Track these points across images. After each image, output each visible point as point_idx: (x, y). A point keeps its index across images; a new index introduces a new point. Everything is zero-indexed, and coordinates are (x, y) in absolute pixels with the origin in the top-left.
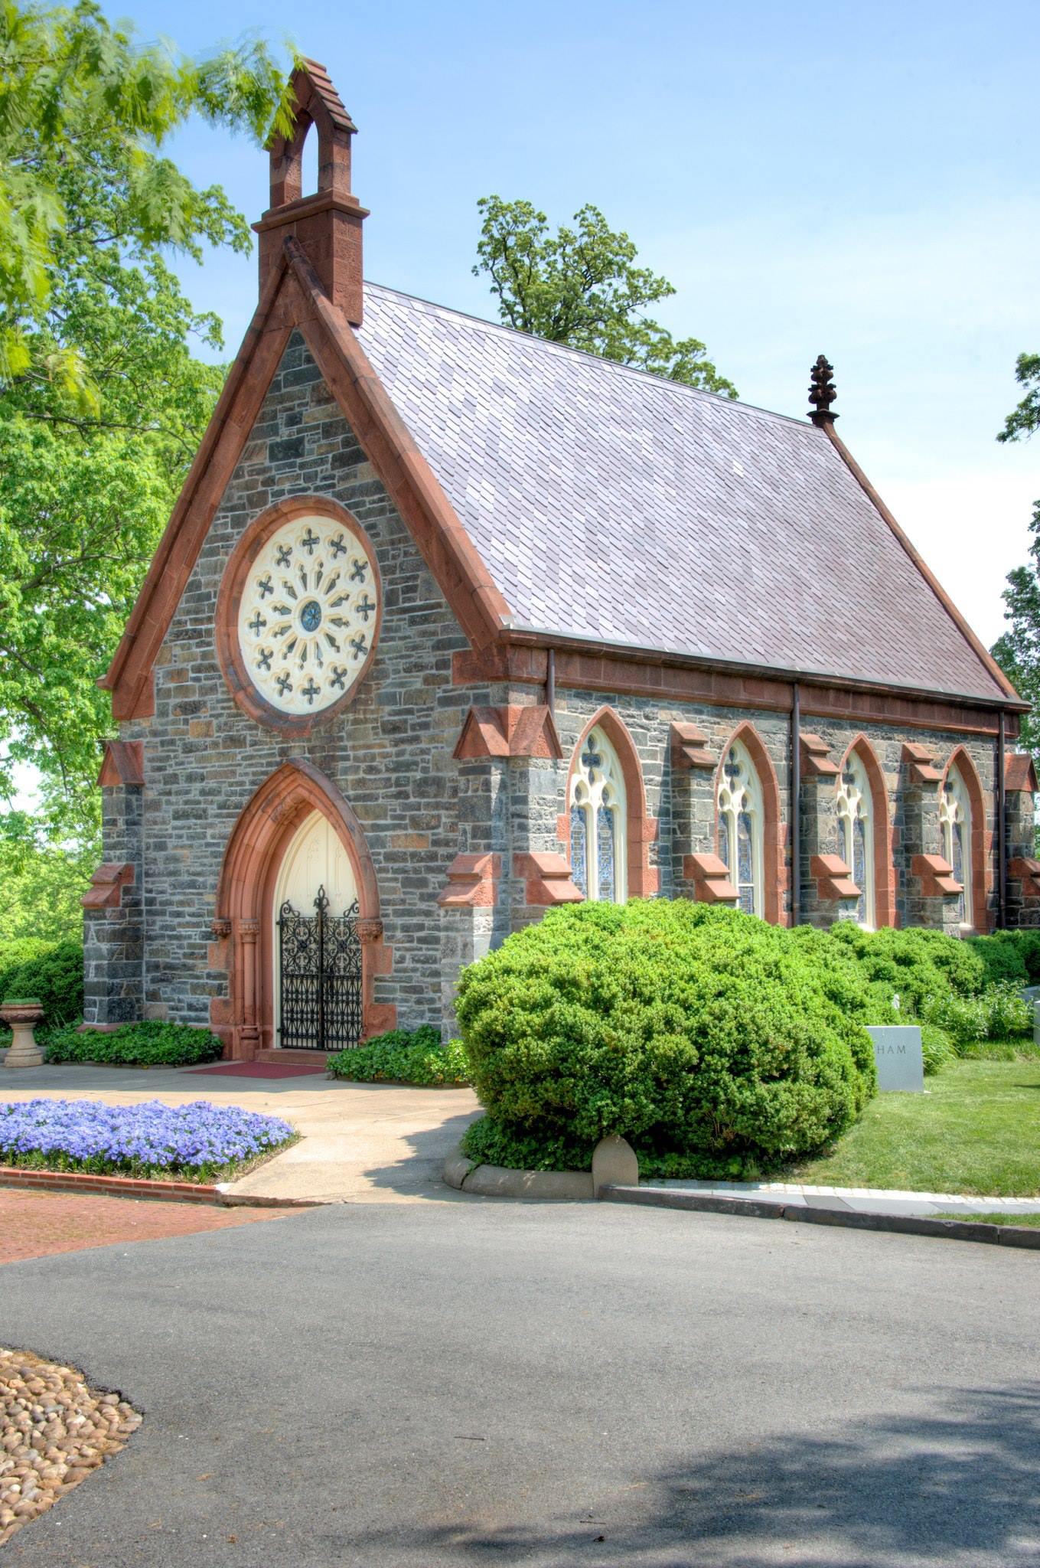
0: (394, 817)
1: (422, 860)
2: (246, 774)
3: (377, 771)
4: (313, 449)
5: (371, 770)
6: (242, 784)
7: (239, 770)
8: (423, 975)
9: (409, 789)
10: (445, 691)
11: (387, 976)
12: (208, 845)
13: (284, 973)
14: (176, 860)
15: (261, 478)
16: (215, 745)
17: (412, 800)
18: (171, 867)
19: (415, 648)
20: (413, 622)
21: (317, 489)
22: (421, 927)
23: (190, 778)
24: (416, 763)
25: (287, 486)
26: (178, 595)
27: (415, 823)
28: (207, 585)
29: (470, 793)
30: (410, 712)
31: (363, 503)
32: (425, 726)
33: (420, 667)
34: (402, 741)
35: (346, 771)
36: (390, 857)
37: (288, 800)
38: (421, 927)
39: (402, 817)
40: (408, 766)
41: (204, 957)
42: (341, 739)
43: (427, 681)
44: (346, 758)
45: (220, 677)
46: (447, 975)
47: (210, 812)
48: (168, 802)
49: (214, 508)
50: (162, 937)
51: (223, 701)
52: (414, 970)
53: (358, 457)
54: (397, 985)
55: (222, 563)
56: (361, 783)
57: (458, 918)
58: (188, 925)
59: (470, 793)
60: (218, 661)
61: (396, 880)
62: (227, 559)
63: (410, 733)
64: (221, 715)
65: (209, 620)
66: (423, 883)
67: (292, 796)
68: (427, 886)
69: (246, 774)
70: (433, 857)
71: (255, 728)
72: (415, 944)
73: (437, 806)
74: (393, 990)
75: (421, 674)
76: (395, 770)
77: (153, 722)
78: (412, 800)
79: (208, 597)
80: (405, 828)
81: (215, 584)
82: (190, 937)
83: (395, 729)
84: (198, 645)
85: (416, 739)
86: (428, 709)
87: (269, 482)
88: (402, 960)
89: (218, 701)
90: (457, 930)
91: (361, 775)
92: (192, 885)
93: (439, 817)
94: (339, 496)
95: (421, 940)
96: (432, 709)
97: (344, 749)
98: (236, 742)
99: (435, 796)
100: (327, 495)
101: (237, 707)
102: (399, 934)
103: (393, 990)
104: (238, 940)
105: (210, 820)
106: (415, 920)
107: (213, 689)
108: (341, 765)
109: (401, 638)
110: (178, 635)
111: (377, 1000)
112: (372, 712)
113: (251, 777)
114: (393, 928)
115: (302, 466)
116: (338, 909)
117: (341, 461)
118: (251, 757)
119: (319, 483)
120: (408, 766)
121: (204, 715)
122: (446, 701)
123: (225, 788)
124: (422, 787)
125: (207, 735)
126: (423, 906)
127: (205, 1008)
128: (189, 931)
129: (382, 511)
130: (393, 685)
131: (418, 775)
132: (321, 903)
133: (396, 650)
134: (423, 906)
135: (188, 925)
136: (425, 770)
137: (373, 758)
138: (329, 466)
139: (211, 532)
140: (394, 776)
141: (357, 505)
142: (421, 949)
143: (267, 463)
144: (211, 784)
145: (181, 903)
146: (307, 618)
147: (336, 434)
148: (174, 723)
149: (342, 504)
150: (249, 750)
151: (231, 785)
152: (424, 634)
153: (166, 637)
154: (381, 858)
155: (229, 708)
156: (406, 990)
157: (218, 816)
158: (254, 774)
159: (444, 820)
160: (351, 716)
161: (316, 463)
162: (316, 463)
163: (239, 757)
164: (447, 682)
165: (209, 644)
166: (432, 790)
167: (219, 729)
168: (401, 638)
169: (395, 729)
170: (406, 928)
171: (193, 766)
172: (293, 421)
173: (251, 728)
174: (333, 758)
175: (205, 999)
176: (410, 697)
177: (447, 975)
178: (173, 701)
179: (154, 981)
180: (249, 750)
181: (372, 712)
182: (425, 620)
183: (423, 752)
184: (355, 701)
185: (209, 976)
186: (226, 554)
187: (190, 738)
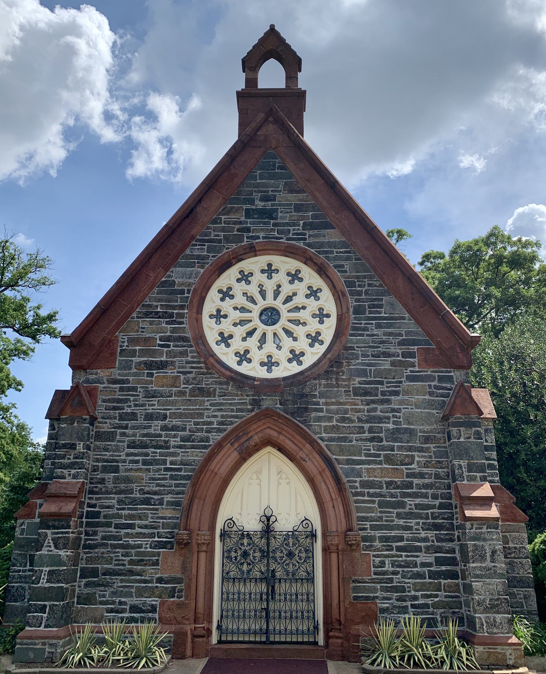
0: (367, 455)
1: (398, 487)
2: (215, 416)
3: (351, 421)
4: (283, 217)
5: (343, 420)
6: (211, 423)
7: (206, 413)
8: (403, 577)
9: (382, 435)
10: (411, 372)
11: (366, 578)
12: (166, 469)
13: (225, 578)
14: (128, 480)
15: (237, 227)
16: (182, 393)
17: (385, 443)
18: (122, 486)
19: (382, 342)
20: (379, 326)
21: (288, 239)
22: (401, 539)
23: (149, 417)
24: (388, 418)
25: (262, 235)
26: (152, 288)
27: (389, 460)
28: (182, 284)
29: (462, 440)
30: (381, 383)
31: (332, 252)
32: (397, 393)
33: (386, 355)
34: (373, 402)
35: (319, 419)
36: (364, 484)
37: (256, 437)
38: (401, 539)
39: (379, 456)
40: (380, 420)
41: (156, 563)
42: (315, 396)
43: (393, 364)
44: (321, 410)
45: (191, 346)
46: (477, 576)
47: (172, 443)
48: (123, 434)
49: (193, 238)
50: (105, 545)
51: (193, 362)
52: (395, 573)
53: (327, 226)
54: (379, 586)
55: (198, 272)
56: (335, 429)
57: (484, 530)
58: (139, 535)
59: (462, 440)
60: (189, 335)
61: (373, 502)
62: (202, 271)
63: (380, 397)
64: (191, 372)
65: (182, 307)
66: (402, 505)
67: (260, 435)
68: (404, 508)
69: (215, 416)
70: (410, 485)
71: (227, 384)
72: (394, 552)
73: (410, 449)
74: (375, 590)
75: (389, 359)
76: (367, 422)
77: (116, 373)
78: (385, 443)
79: (182, 292)
80: (380, 463)
81: (190, 285)
82: (140, 546)
83: (366, 393)
84: (167, 323)
85: (388, 401)
86: (396, 382)
87: (248, 230)
88: (383, 564)
89: (188, 362)
90: (485, 540)
91: (335, 423)
92: (146, 502)
93: (413, 457)
94: (309, 245)
95: (399, 549)
96: (401, 382)
97: (318, 404)
98: (202, 392)
99: (408, 442)
100: (301, 244)
101: (207, 368)
102: (377, 544)
103: (375, 590)
104: (195, 548)
105: (172, 450)
106: (393, 533)
107: (184, 354)
108: (313, 414)
109: (367, 335)
110: (147, 315)
111: (355, 598)
112: (344, 380)
113: (219, 419)
114: (371, 539)
115: (275, 225)
116: (285, 523)
117: (308, 226)
118: (222, 404)
119: (291, 235)
120: (380, 420)
121: (170, 372)
122: (411, 378)
123: (191, 425)
124: (394, 435)
125: (173, 386)
126: (401, 522)
127: (153, 609)
128: (139, 541)
129: (348, 259)
130: (363, 364)
131: (391, 426)
132: (267, 520)
133: (364, 342)
134: (401, 522)
135: (139, 535)
136: (394, 423)
137: (346, 411)
138: (301, 228)
139: (188, 252)
140: (367, 426)
141: (326, 252)
142: (401, 556)
143: (243, 219)
144: (176, 422)
145: (131, 517)
146: (264, 317)
147: (306, 211)
148: (135, 375)
149: (313, 251)
150: (217, 399)
151: (196, 424)
152: (390, 334)
153: (134, 315)
154: (357, 484)
155: (200, 368)
156: (383, 589)
157: (180, 447)
158: (222, 416)
159: (417, 459)
160: (323, 382)
161: (288, 224)
162: (288, 224)
163: (207, 403)
164: (414, 366)
165: (182, 323)
166: (406, 437)
167: (187, 382)
168: (367, 335)
169: (366, 393)
170: (383, 539)
171: (154, 406)
172: (265, 199)
173: (221, 383)
174: (306, 409)
175: (154, 601)
176: (378, 373)
177: (477, 576)
178: (136, 359)
179: (87, 585)
180: (217, 399)
181: (344, 380)
182: (390, 326)
183: (393, 410)
184: (327, 372)
185: (160, 580)
186: (202, 267)
187: (153, 387)
